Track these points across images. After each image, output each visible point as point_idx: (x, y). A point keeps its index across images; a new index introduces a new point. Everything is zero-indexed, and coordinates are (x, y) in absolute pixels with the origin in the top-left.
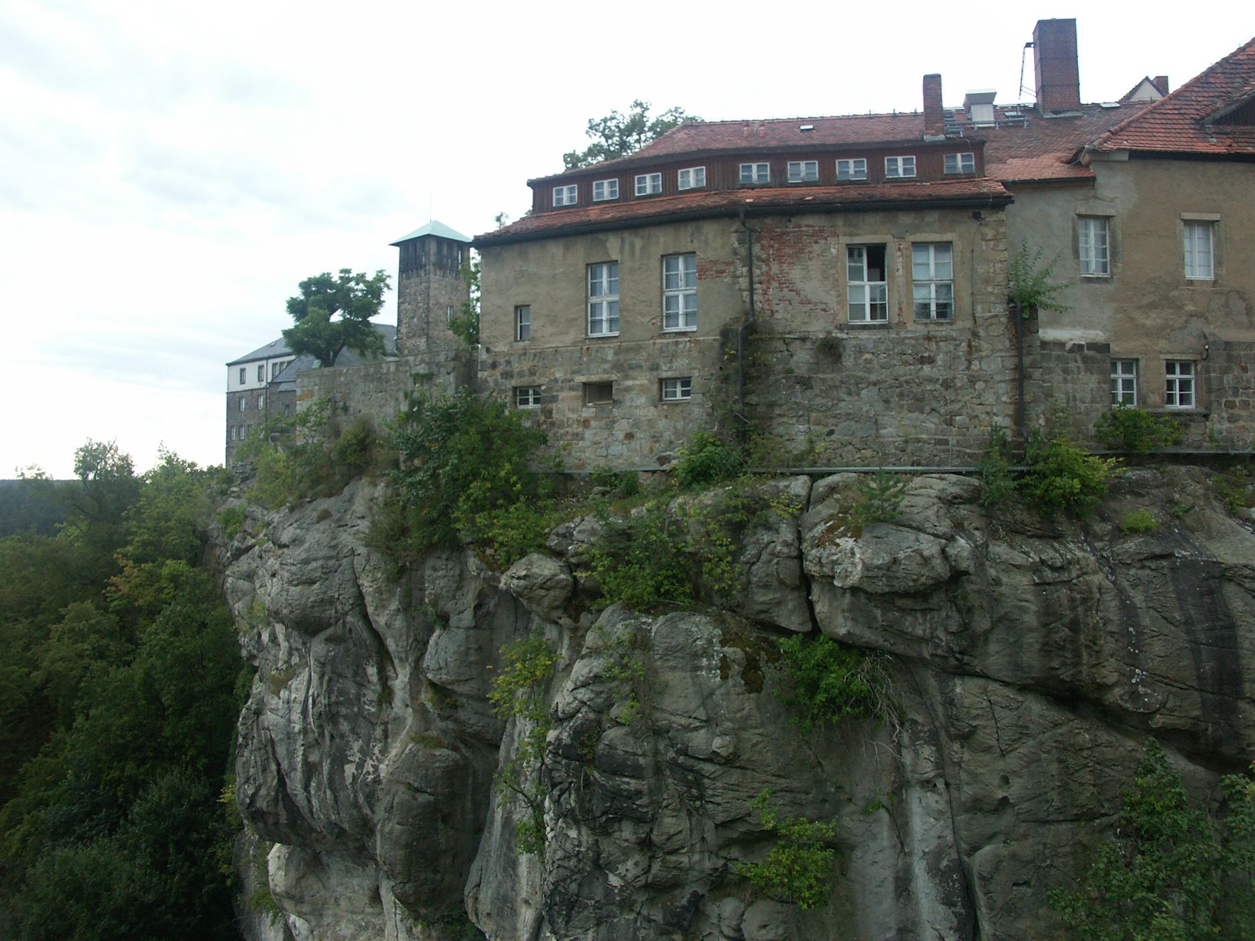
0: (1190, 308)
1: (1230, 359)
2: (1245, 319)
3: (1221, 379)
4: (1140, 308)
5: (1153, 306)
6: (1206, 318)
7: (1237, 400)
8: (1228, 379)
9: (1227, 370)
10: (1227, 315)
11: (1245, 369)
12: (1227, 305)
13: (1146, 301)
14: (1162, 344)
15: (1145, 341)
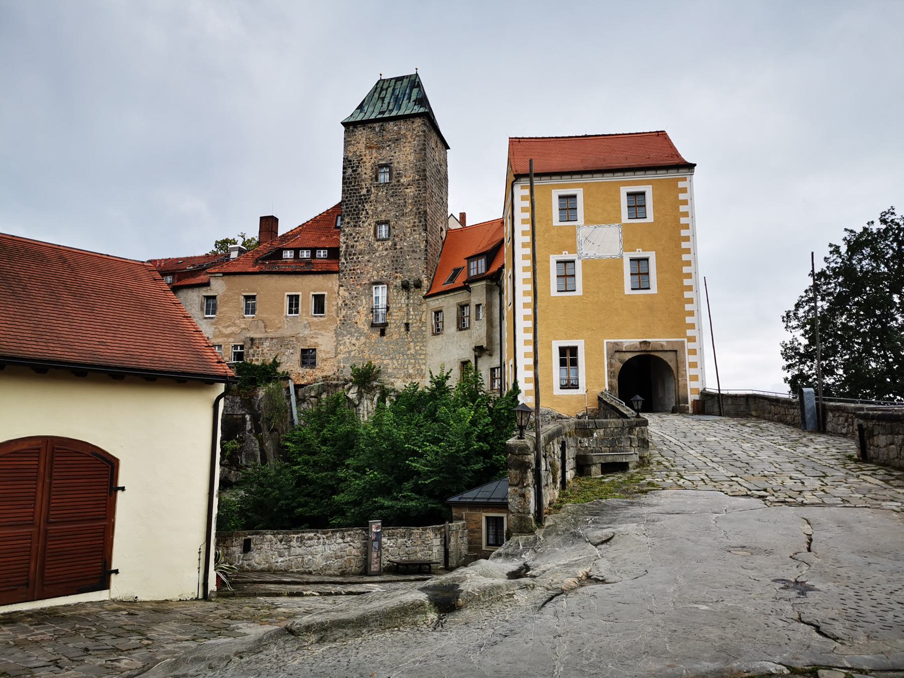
0: (243, 326)
1: (252, 344)
2: (264, 330)
3: (248, 352)
4: (223, 327)
5: (229, 326)
6: (249, 330)
7: (254, 359)
8: (251, 351)
9: (251, 348)
10: (257, 328)
11: (258, 348)
12: (257, 325)
13: (226, 325)
14: (231, 340)
15: (225, 339)
